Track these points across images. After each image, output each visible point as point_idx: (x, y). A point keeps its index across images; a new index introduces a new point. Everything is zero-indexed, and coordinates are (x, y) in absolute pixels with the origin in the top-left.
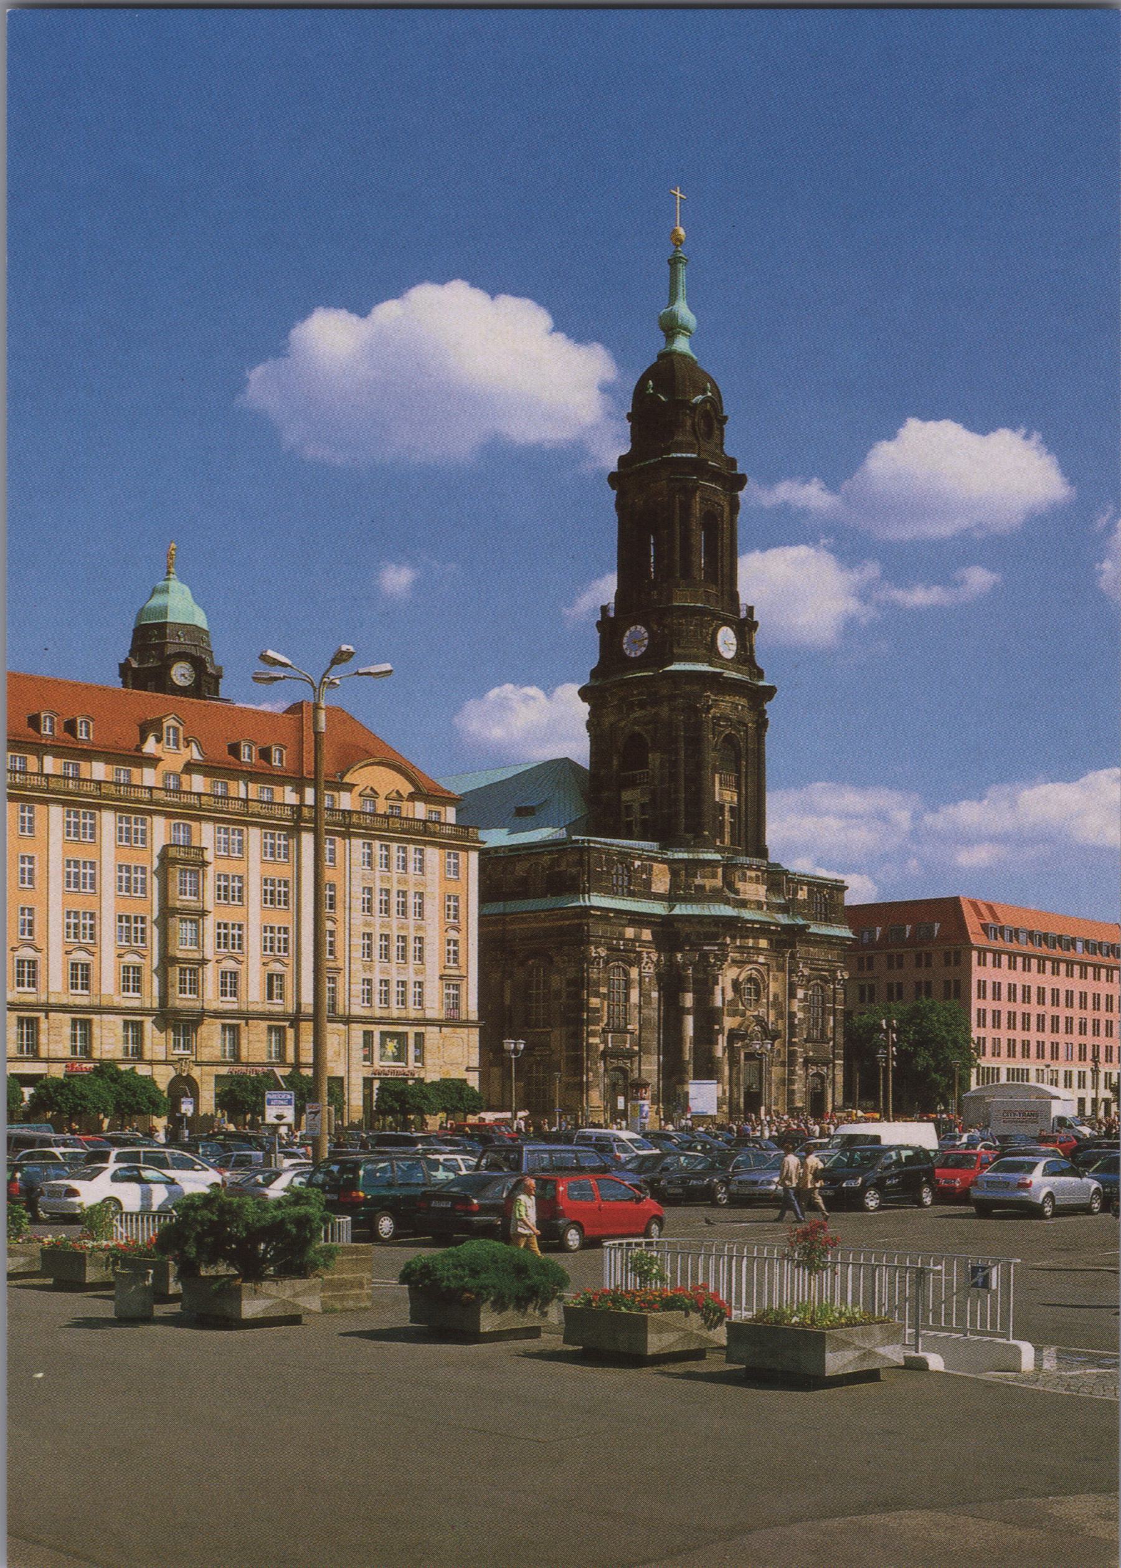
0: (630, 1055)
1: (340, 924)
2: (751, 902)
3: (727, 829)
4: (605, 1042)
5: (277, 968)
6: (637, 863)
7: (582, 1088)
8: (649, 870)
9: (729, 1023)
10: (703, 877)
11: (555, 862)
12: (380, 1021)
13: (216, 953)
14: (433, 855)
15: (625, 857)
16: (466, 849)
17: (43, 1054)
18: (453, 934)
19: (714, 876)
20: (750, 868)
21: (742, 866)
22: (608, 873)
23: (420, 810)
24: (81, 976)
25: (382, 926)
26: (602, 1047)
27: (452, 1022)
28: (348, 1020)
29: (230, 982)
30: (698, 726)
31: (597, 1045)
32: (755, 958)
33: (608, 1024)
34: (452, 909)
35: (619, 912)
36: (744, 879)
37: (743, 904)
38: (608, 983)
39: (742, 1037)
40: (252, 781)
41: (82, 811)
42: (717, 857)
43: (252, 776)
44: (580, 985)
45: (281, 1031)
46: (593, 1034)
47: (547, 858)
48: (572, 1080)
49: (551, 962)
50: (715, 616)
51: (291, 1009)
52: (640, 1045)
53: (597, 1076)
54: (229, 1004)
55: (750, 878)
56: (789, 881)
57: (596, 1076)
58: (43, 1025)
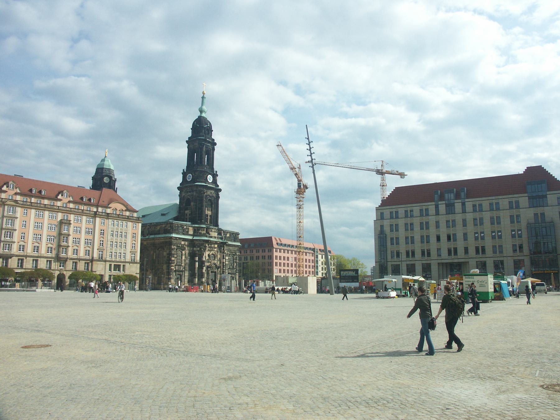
0: (182, 271)
1: (105, 239)
2: (213, 237)
3: (209, 220)
4: (176, 268)
5: (88, 249)
6: (185, 227)
7: (169, 279)
9: (207, 264)
11: (165, 226)
12: (113, 262)
13: (72, 245)
14: (130, 224)
15: (182, 226)
16: (139, 223)
17: (24, 267)
18: (134, 242)
19: (204, 231)
20: (213, 229)
21: (211, 228)
23: (128, 213)
24: (36, 249)
25: (115, 240)
26: (175, 269)
27: (133, 262)
28: (105, 261)
30: (202, 197)
33: (177, 264)
34: (134, 236)
35: (180, 238)
36: (211, 231)
37: (211, 237)
39: (210, 268)
40: (85, 205)
41: (53, 213)
42: (205, 226)
44: (170, 255)
45: (88, 264)
46: (173, 266)
47: (164, 225)
48: (168, 277)
49: (164, 249)
50: (207, 172)
52: (185, 269)
53: (173, 276)
54: (75, 256)
56: (224, 232)
57: (173, 276)
58: (25, 260)
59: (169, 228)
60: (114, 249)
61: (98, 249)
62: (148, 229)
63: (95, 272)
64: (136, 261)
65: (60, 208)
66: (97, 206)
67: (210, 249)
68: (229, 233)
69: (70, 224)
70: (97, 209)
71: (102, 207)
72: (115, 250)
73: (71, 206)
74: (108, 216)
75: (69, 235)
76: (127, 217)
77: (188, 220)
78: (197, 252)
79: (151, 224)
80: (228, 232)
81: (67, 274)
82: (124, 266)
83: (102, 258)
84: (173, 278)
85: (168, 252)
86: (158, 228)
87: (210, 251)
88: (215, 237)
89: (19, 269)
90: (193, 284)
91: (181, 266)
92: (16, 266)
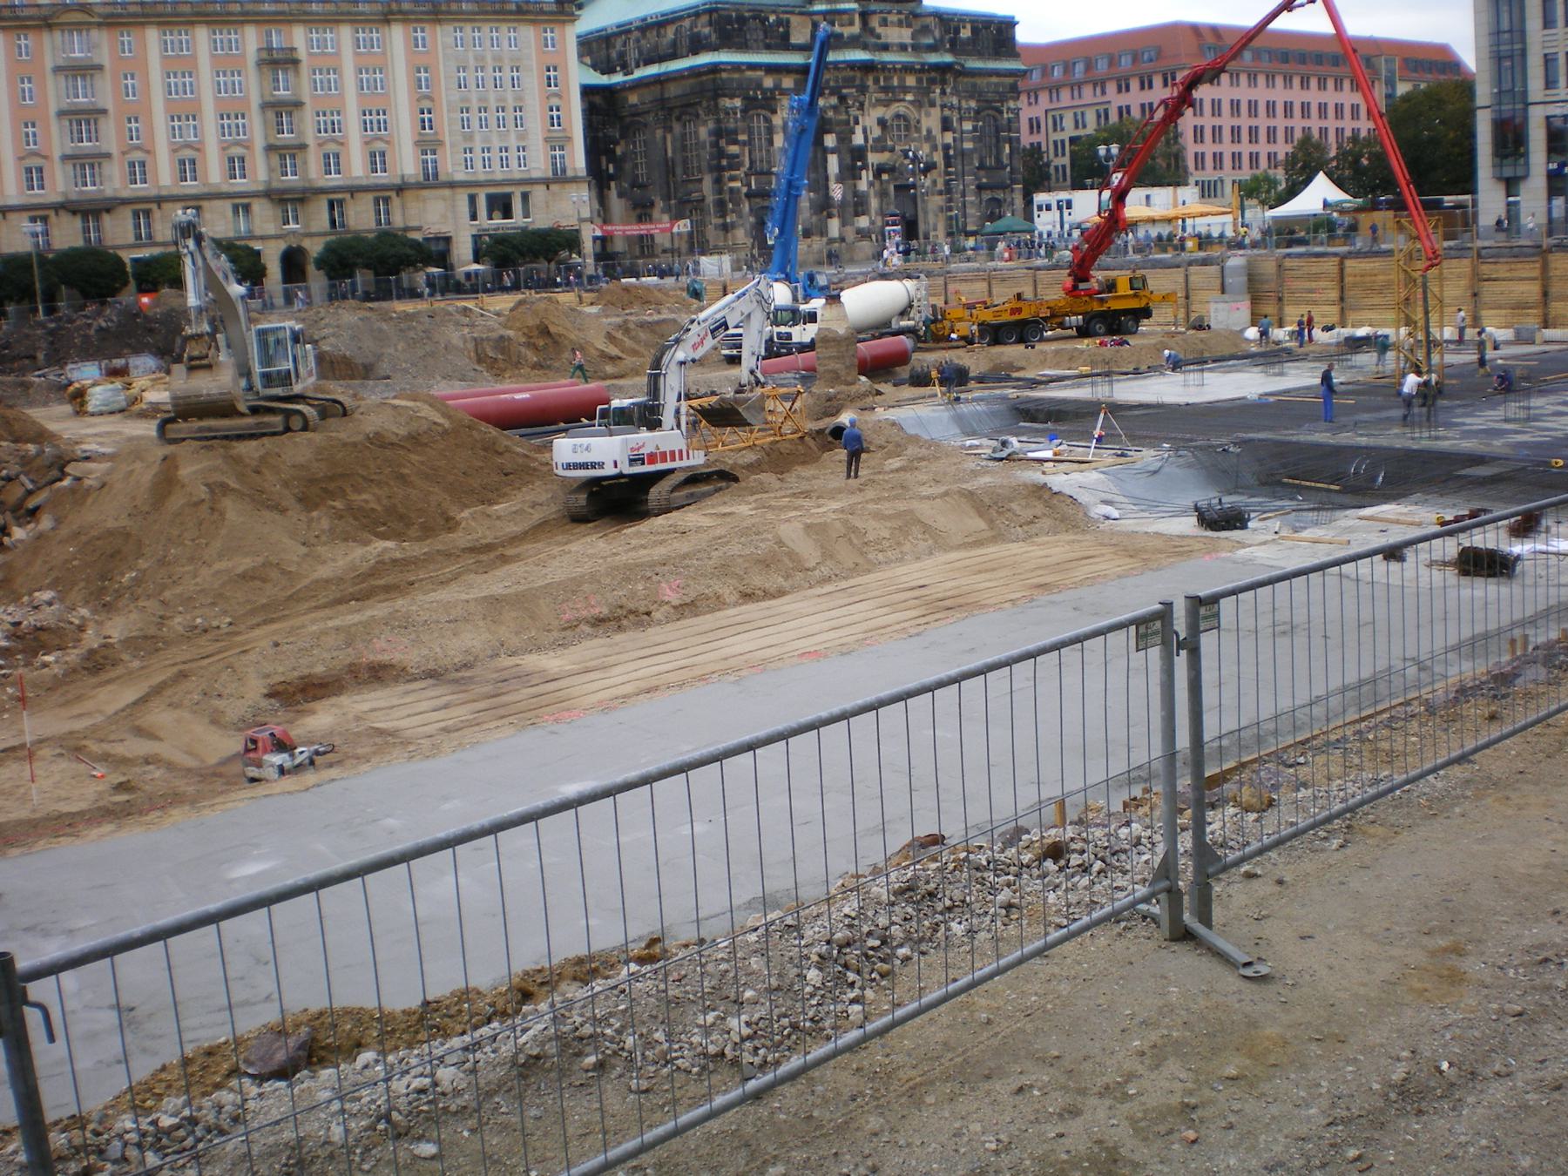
4: (749, 185)
6: (772, 18)
9: (873, 158)
10: (841, 25)
17: (159, 238)
19: (851, 23)
22: (740, 29)
24: (188, 168)
26: (745, 190)
27: (559, 177)
29: (332, 162)
31: (738, 190)
32: (902, 96)
33: (750, 168)
35: (753, 67)
36: (884, 23)
37: (885, 48)
38: (750, 132)
46: (733, 179)
47: (687, 23)
48: (720, 221)
49: (697, 116)
51: (398, 181)
54: (334, 180)
58: (157, 214)
59: (706, 30)
60: (477, 137)
61: (417, 143)
62: (638, 41)
63: (419, 229)
64: (570, 173)
67: (882, 96)
68: (972, 22)
69: (296, 62)
72: (486, 139)
75: (298, 105)
78: (830, 114)
79: (644, 19)
80: (964, 21)
81: (314, 248)
82: (525, 197)
83: (436, 175)
85: (711, 125)
87: (886, 104)
88: (903, 48)
89: (145, 246)
90: (825, 239)
91: (770, 173)
92: (131, 239)
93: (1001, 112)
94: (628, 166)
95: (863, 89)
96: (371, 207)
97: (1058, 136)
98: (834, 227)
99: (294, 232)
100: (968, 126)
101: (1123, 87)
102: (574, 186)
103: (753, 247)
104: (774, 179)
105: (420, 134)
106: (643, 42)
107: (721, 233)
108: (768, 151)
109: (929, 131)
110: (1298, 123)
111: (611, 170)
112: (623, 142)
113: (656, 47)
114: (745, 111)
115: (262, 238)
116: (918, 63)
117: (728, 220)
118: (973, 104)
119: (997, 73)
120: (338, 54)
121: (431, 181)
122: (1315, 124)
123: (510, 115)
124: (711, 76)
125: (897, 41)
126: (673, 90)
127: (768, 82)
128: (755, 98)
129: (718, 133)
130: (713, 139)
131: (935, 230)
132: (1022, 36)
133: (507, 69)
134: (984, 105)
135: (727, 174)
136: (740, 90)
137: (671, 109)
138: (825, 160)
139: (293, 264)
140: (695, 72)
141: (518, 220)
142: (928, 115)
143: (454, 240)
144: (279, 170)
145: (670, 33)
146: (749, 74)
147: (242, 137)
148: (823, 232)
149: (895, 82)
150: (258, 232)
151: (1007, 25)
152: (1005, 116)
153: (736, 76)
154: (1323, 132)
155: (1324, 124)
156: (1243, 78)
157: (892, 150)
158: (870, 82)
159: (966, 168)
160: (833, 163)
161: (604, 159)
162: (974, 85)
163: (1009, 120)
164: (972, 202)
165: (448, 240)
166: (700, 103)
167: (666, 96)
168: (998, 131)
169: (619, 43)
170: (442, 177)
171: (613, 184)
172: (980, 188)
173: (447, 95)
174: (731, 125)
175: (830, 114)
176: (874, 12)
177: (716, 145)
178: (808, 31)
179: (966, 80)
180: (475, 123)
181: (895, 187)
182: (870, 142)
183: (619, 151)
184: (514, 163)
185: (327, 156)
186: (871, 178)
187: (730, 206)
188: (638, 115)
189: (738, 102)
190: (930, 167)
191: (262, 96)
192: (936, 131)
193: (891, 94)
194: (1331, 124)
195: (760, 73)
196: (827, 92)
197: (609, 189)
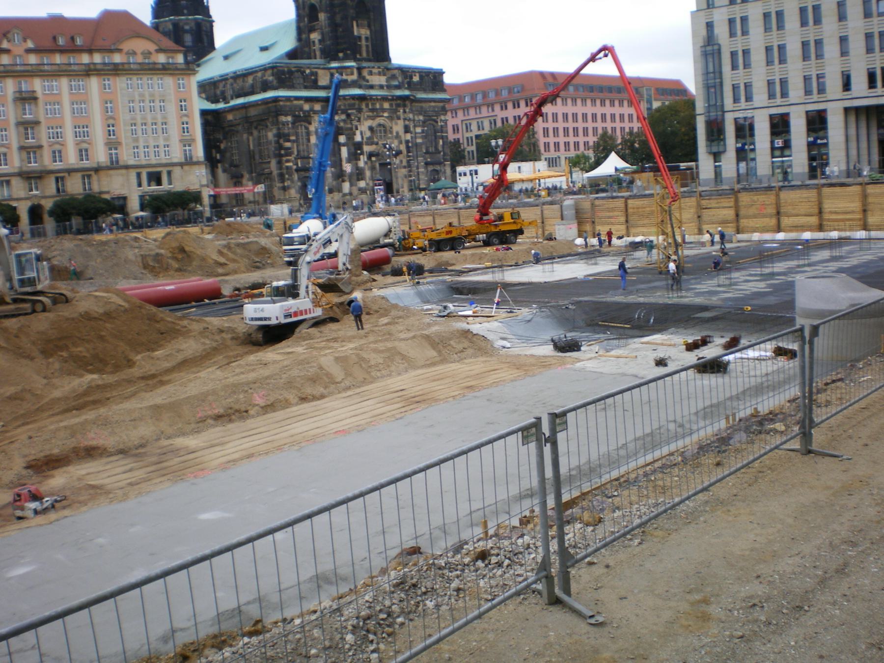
3: (364, 49)
4: (297, 164)
6: (308, 71)
8: (316, 74)
9: (367, 149)
10: (347, 75)
11: (264, 75)
19: (352, 74)
22: (290, 78)
26: (295, 167)
27: (189, 162)
29: (57, 155)
32: (381, 114)
33: (298, 155)
36: (371, 73)
37: (372, 87)
38: (297, 135)
43: (62, 51)
46: (288, 161)
47: (259, 74)
48: (281, 185)
49: (267, 127)
51: (95, 165)
54: (58, 165)
55: (375, 73)
59: (271, 78)
61: (107, 144)
62: (232, 85)
63: (108, 192)
64: (195, 159)
65: (9, 68)
66: (90, 51)
67: (370, 114)
68: (419, 72)
70: (92, 57)
71: (99, 51)
73: (33, 59)
74: (116, 70)
75: (37, 123)
76: (160, 66)
77: (318, 53)
79: (235, 73)
80: (415, 72)
81: (48, 204)
82: (169, 173)
83: (117, 162)
84: (294, 187)
85: (275, 131)
86: (250, 80)
87: (373, 118)
88: (381, 87)
90: (341, 194)
93: (437, 122)
94: (228, 155)
95: (360, 110)
96: (80, 181)
97: (469, 135)
98: (346, 186)
99: (36, 196)
100: (419, 130)
101: (504, 107)
102: (197, 167)
103: (300, 199)
104: (311, 161)
105: (108, 139)
106: (235, 85)
107: (282, 192)
108: (307, 146)
109: (397, 133)
110: (600, 125)
111: (218, 156)
112: (224, 142)
113: (242, 88)
114: (293, 123)
115: (18, 199)
116: (390, 96)
117: (286, 184)
118: (421, 118)
119: (434, 100)
120: (59, 94)
121: (115, 165)
122: (609, 125)
123: (159, 127)
124: (274, 104)
125: (377, 83)
126: (253, 112)
127: (307, 107)
128: (299, 116)
129: (279, 136)
130: (276, 139)
131: (403, 188)
132: (447, 79)
133: (157, 102)
134: (427, 118)
135: (284, 159)
136: (291, 112)
137: (251, 123)
138: (340, 150)
139: (36, 214)
140: (265, 102)
141: (165, 186)
142: (396, 124)
143: (129, 198)
144: (27, 160)
145: (250, 80)
146: (296, 102)
147: (5, 142)
148: (340, 190)
149: (378, 106)
150: (15, 196)
151: (439, 74)
152: (439, 124)
153: (288, 104)
154: (614, 129)
155: (614, 125)
156: (569, 101)
157: (377, 144)
158: (364, 106)
159: (419, 153)
160: (344, 152)
161: (214, 151)
162: (422, 107)
163: (442, 126)
164: (422, 172)
165: (125, 198)
166: (268, 119)
167: (249, 115)
168: (436, 132)
169: (221, 85)
170: (121, 163)
171: (219, 165)
172: (427, 164)
173: (123, 116)
174: (286, 131)
175: (342, 124)
176: (365, 68)
177: (278, 142)
178: (328, 78)
179: (417, 104)
180: (140, 132)
181: (381, 165)
182: (365, 139)
183: (222, 146)
184: (162, 155)
185: (54, 152)
186: (366, 160)
187: (287, 176)
188: (232, 126)
189: (289, 118)
190: (399, 153)
191: (16, 118)
192: (402, 133)
193: (376, 113)
194: (618, 125)
195: (302, 102)
196: (339, 112)
197: (217, 168)
